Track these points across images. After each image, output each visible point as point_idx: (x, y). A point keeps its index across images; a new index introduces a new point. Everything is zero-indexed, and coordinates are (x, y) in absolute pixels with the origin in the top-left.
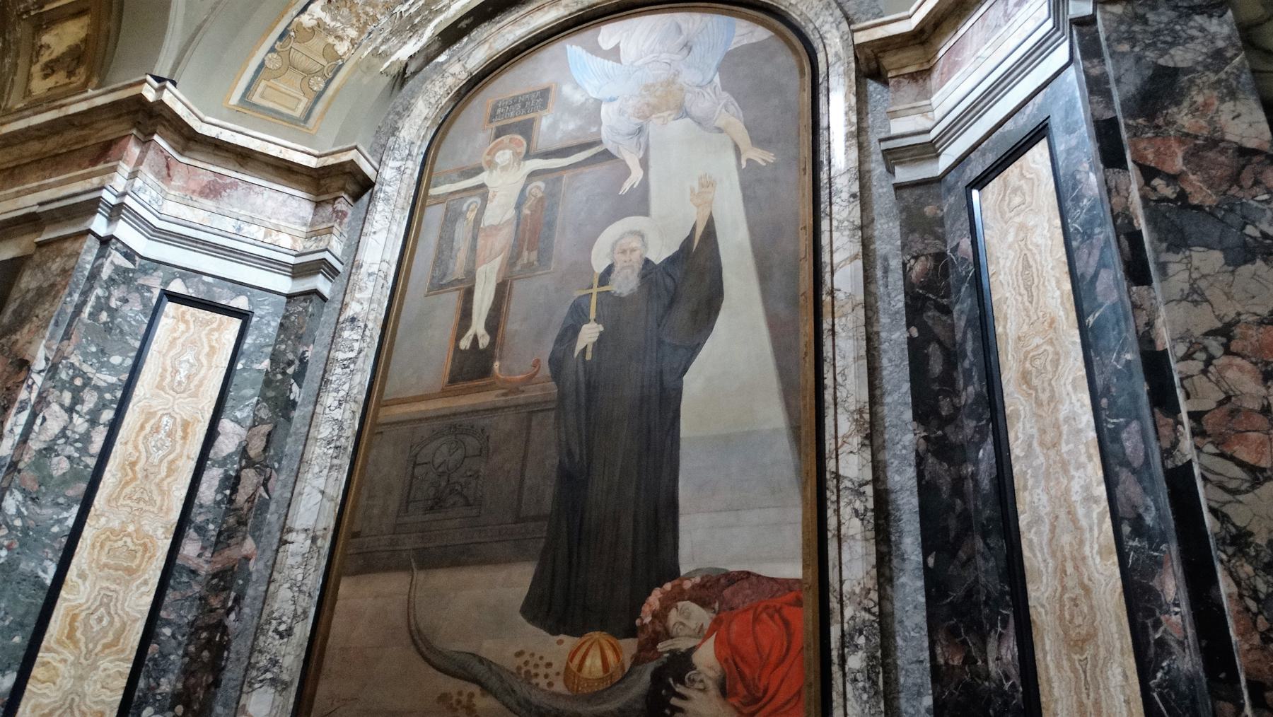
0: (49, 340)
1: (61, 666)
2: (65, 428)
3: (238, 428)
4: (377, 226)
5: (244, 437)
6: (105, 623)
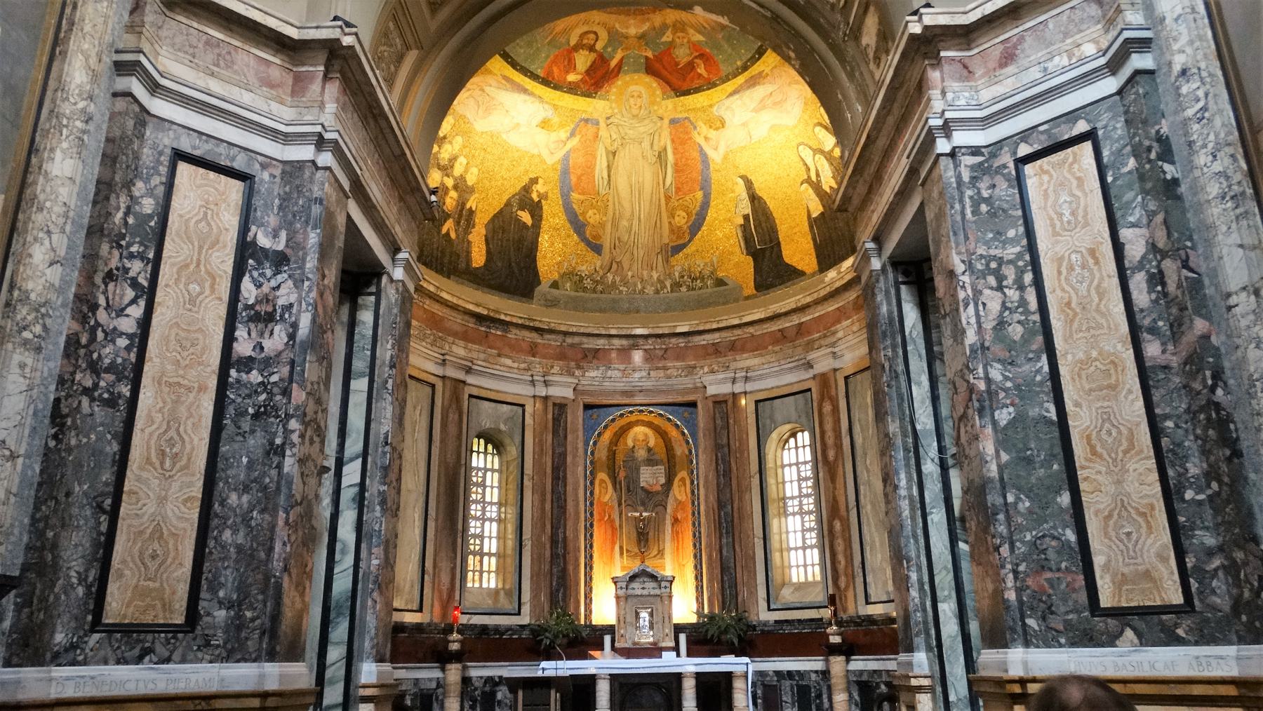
0: (957, 248)
1: (1099, 477)
2: (1004, 303)
3: (1137, 230)
5: (1148, 235)
6: (1114, 434)
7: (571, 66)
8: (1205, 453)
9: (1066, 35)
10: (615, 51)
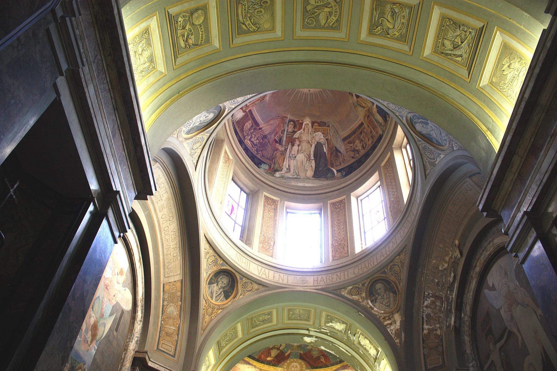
7: (269, 354)
10: (288, 350)
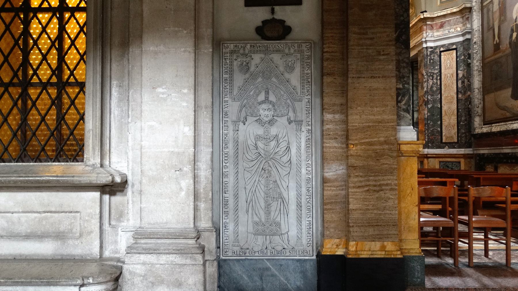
2: (433, 83)
4: (475, 18)
8: (465, 116)
9: (455, 25)
